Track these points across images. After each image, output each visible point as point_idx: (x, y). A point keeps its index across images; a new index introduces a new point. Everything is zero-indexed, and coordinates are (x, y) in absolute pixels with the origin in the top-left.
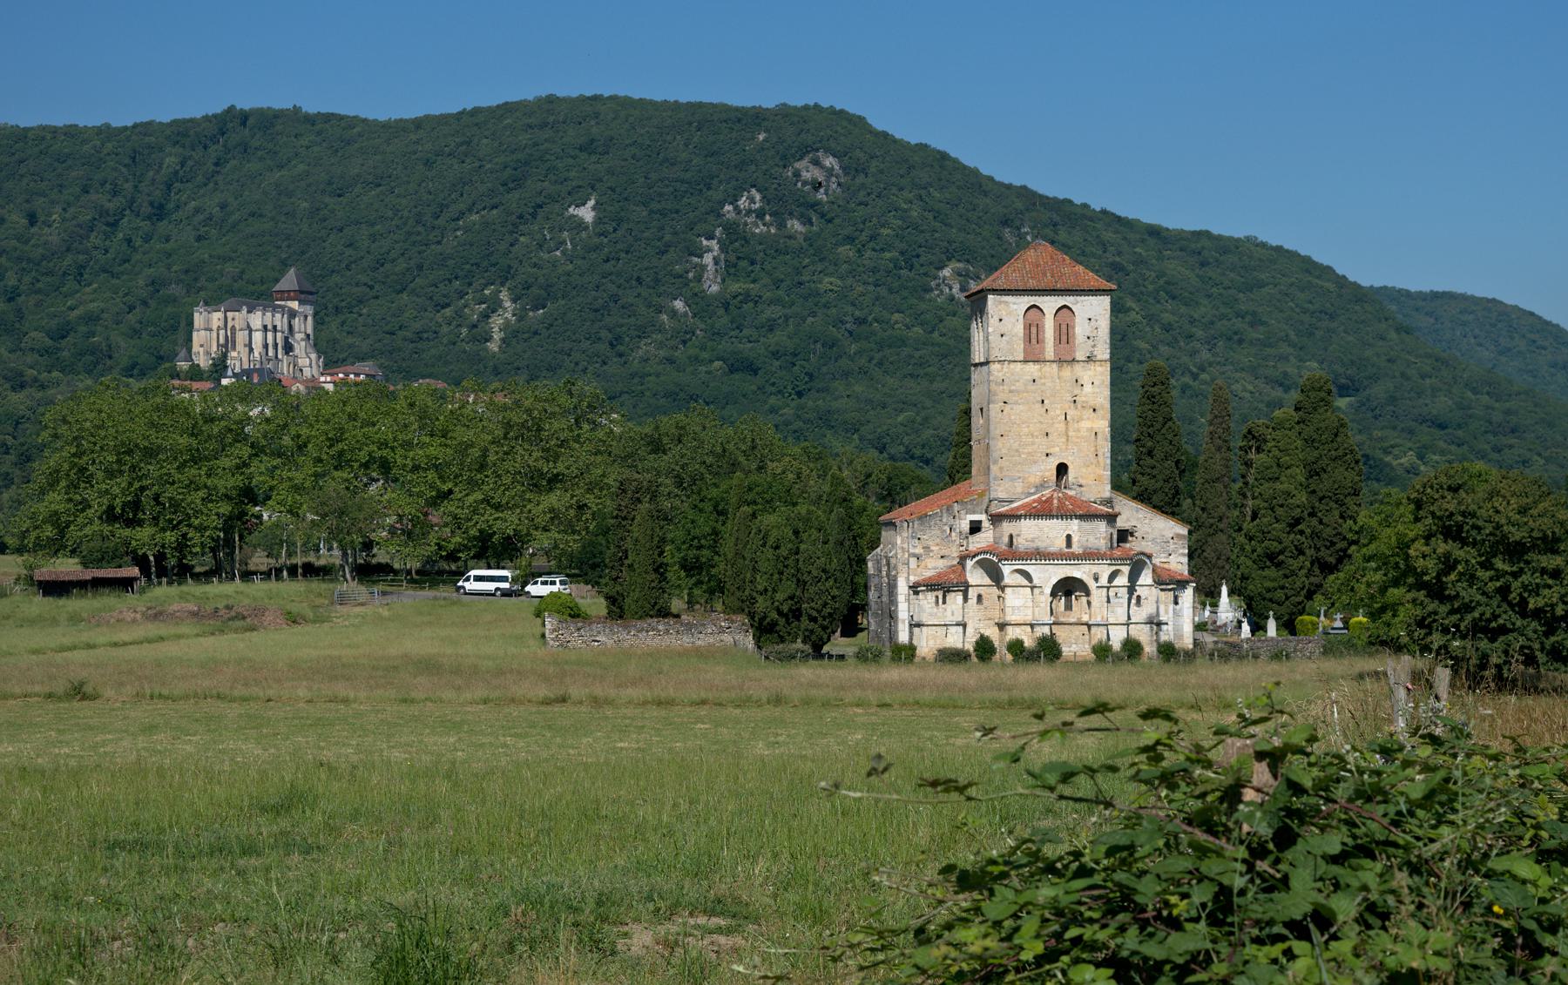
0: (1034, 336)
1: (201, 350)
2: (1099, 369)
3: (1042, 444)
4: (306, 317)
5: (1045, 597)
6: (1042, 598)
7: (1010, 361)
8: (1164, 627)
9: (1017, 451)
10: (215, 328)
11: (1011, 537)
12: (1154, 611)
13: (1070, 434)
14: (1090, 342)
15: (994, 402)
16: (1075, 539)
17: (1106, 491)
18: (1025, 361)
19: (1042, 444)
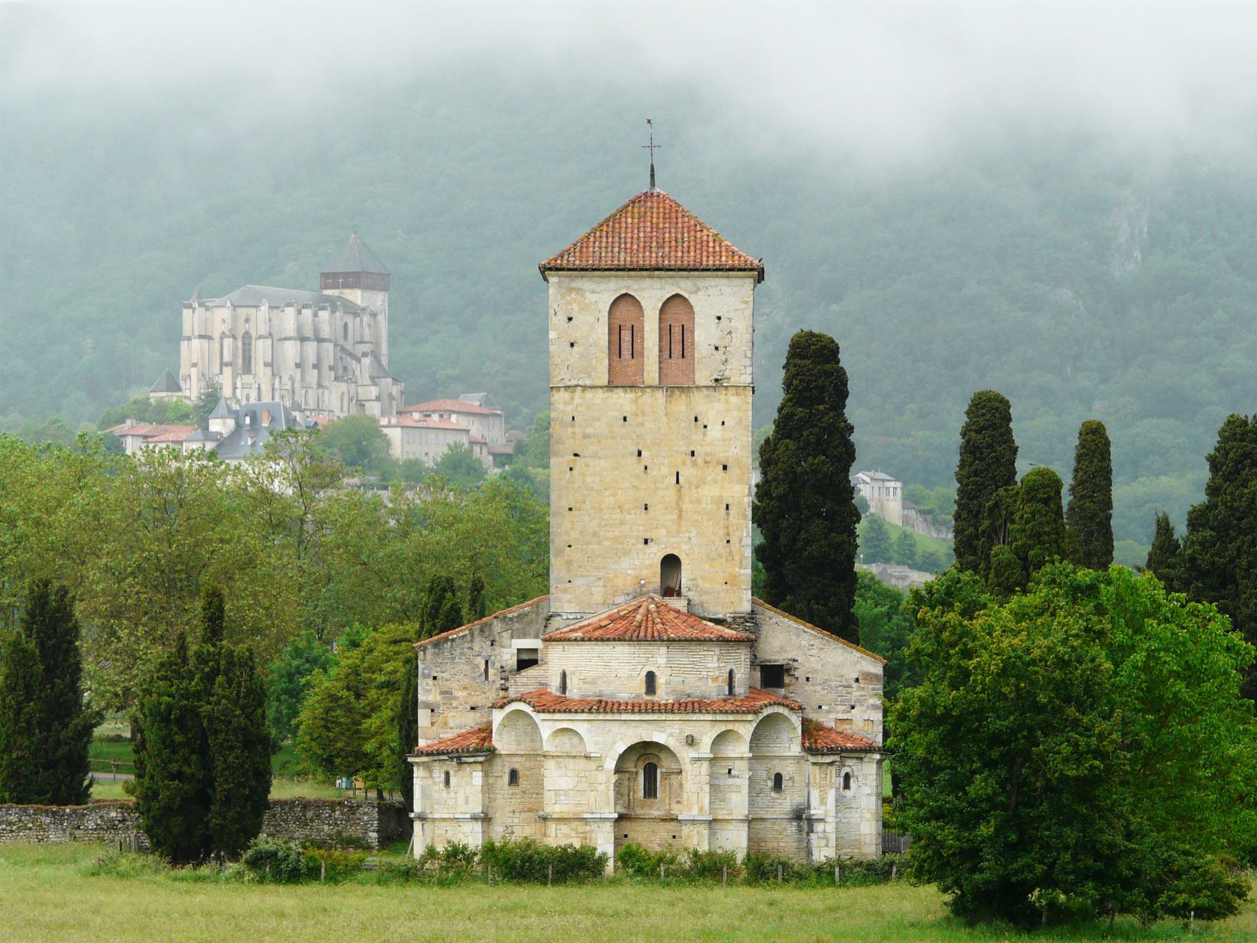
0: (626, 345)
1: (194, 371)
2: (734, 399)
3: (637, 524)
4: (374, 315)
5: (606, 778)
6: (601, 777)
7: (585, 388)
8: (819, 827)
9: (595, 534)
10: (217, 335)
11: (564, 675)
12: (803, 800)
13: (685, 506)
14: (719, 356)
15: (557, 454)
16: (661, 680)
17: (743, 601)
18: (611, 386)
19: (637, 524)
